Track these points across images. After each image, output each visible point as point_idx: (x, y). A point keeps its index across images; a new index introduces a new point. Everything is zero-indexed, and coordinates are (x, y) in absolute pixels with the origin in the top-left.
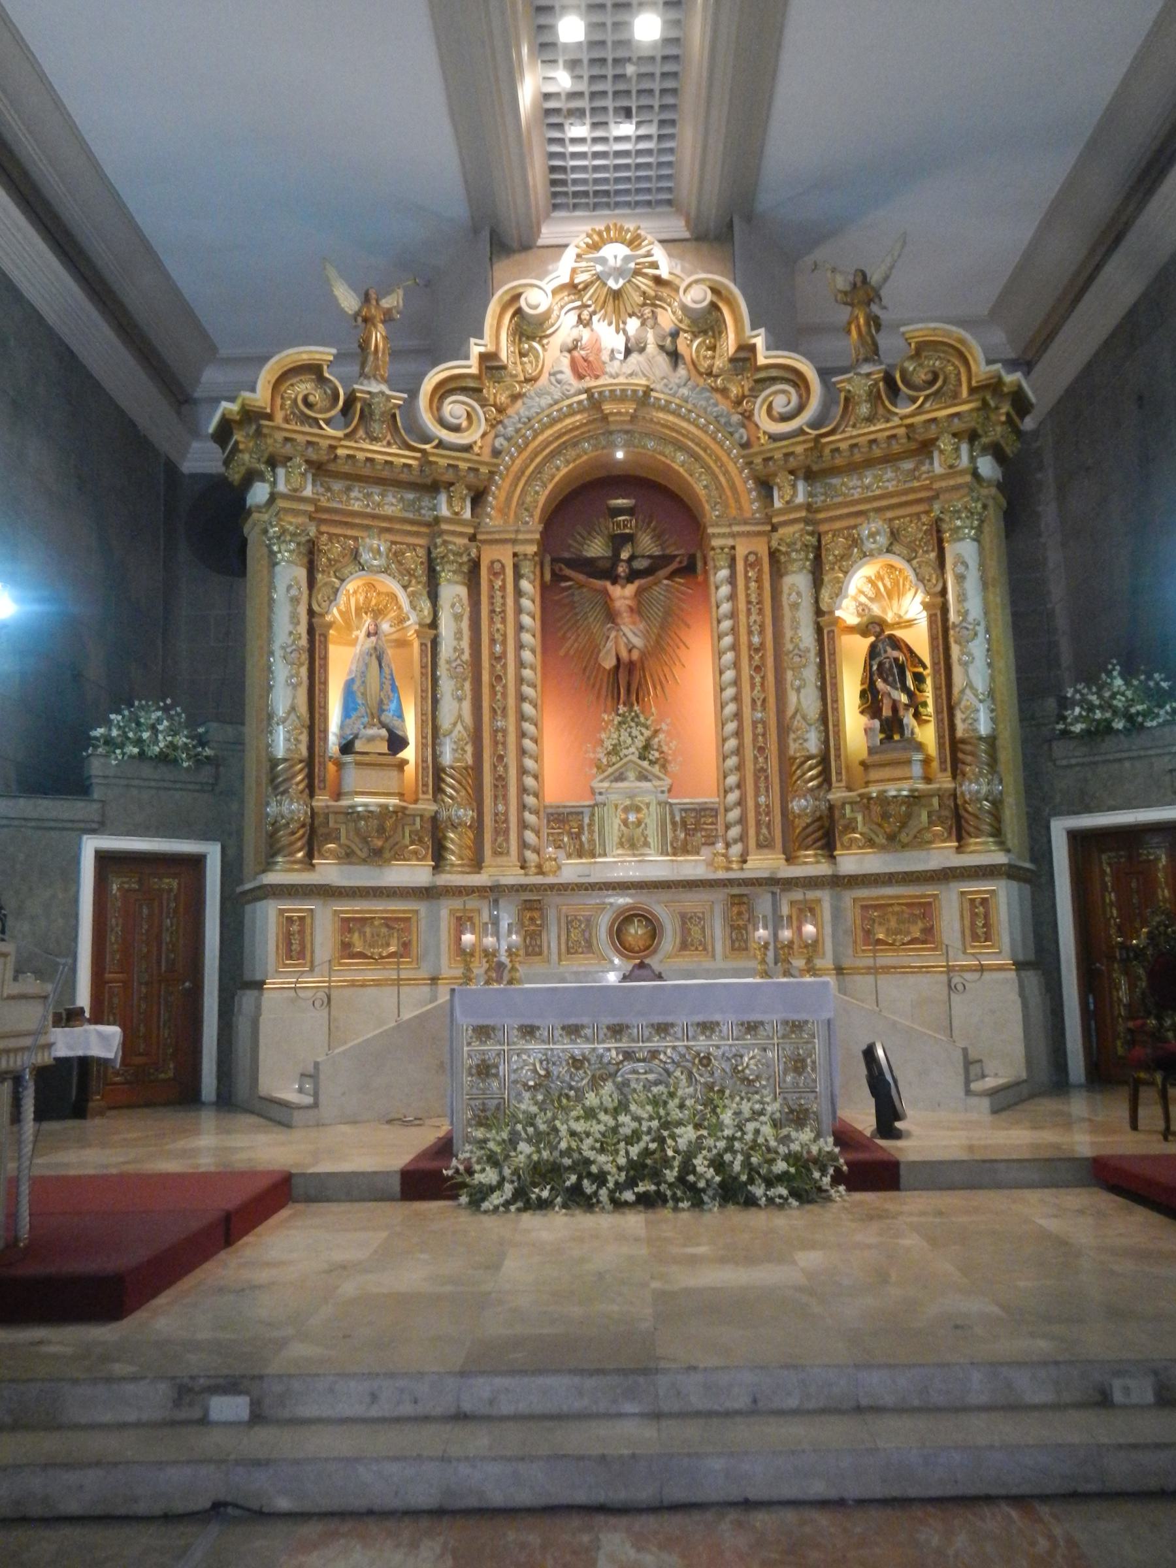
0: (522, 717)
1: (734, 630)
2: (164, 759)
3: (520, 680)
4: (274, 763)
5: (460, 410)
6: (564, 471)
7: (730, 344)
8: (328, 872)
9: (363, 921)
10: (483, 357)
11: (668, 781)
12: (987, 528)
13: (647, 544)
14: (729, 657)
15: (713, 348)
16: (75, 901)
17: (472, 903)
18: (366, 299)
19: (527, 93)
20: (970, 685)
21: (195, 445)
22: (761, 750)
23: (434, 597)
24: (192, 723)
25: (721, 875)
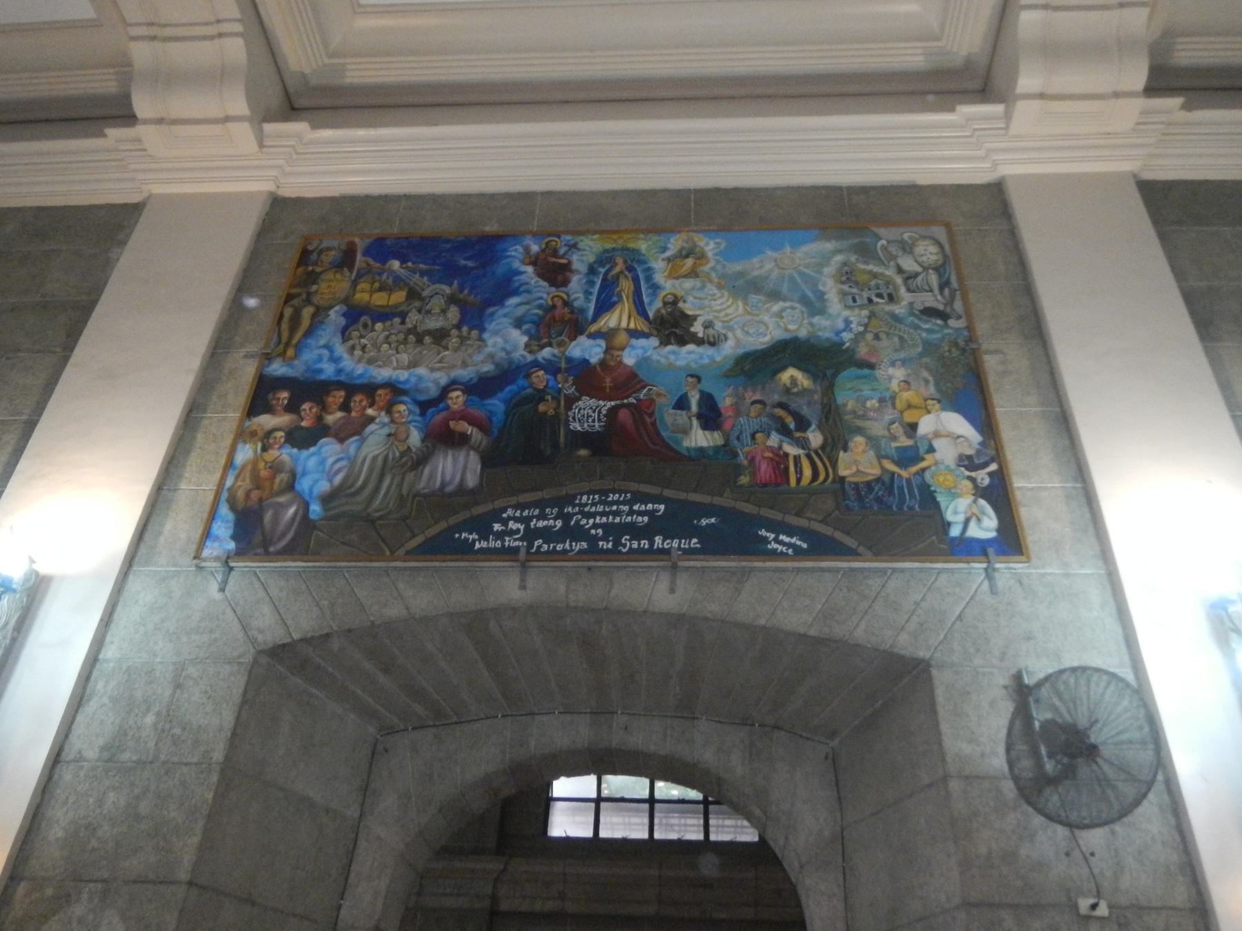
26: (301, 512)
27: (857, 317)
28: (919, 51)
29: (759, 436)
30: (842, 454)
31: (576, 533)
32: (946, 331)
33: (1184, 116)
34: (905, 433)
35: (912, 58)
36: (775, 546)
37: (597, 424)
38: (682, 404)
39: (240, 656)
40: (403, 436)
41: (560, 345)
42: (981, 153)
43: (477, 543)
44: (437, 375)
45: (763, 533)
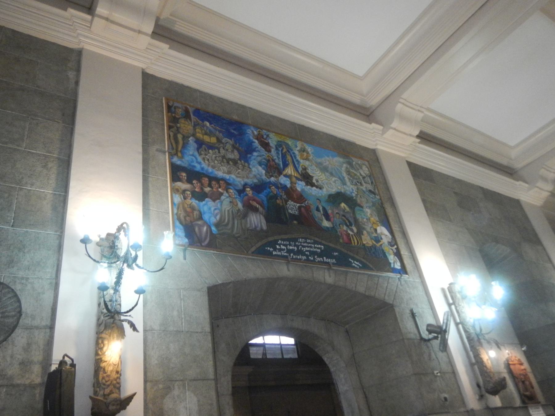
26: (209, 229)
27: (355, 188)
28: (359, 98)
29: (341, 225)
30: (362, 236)
31: (300, 252)
32: (376, 199)
33: (418, 144)
34: (375, 232)
35: (356, 99)
36: (354, 265)
37: (296, 212)
38: (318, 209)
39: (202, 288)
40: (235, 204)
41: (276, 177)
42: (374, 139)
43: (273, 252)
44: (239, 179)
45: (350, 260)
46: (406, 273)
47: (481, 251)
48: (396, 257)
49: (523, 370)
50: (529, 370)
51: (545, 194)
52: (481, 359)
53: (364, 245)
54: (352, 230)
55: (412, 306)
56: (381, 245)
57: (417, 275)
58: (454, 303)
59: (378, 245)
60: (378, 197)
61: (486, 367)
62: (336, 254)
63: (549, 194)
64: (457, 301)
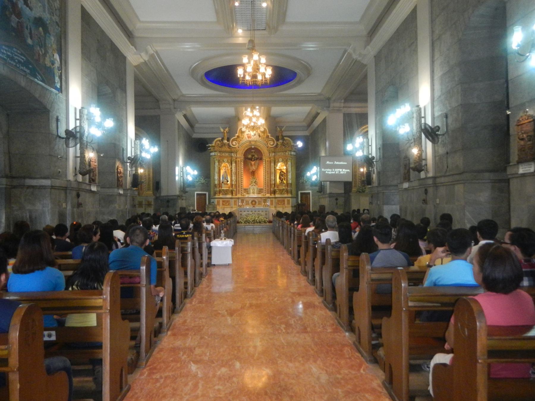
0: (241, 178)
1: (265, 169)
2: (203, 183)
3: (241, 174)
4: (215, 184)
5: (235, 143)
6: (246, 149)
7: (266, 135)
8: (221, 196)
9: (225, 201)
10: (237, 136)
11: (257, 186)
12: (292, 160)
13: (256, 156)
14: (265, 172)
15: (264, 135)
16: (195, 199)
17: (236, 199)
18: (224, 130)
19: (243, 114)
20: (289, 178)
21: (194, 134)
22: (268, 183)
23: (232, 165)
24: (204, 179)
25: (263, 197)
31: (12, 59)
36: (38, 77)
46: (62, 92)
47: (98, 88)
48: (59, 79)
49: (95, 165)
50: (97, 166)
51: (142, 61)
52: (85, 156)
53: (45, 64)
54: (42, 51)
55: (58, 115)
56: (54, 67)
57: (65, 94)
58: (80, 120)
59: (52, 67)
60: (60, 29)
61: (85, 160)
62: (31, 66)
63: (144, 61)
64: (83, 119)
